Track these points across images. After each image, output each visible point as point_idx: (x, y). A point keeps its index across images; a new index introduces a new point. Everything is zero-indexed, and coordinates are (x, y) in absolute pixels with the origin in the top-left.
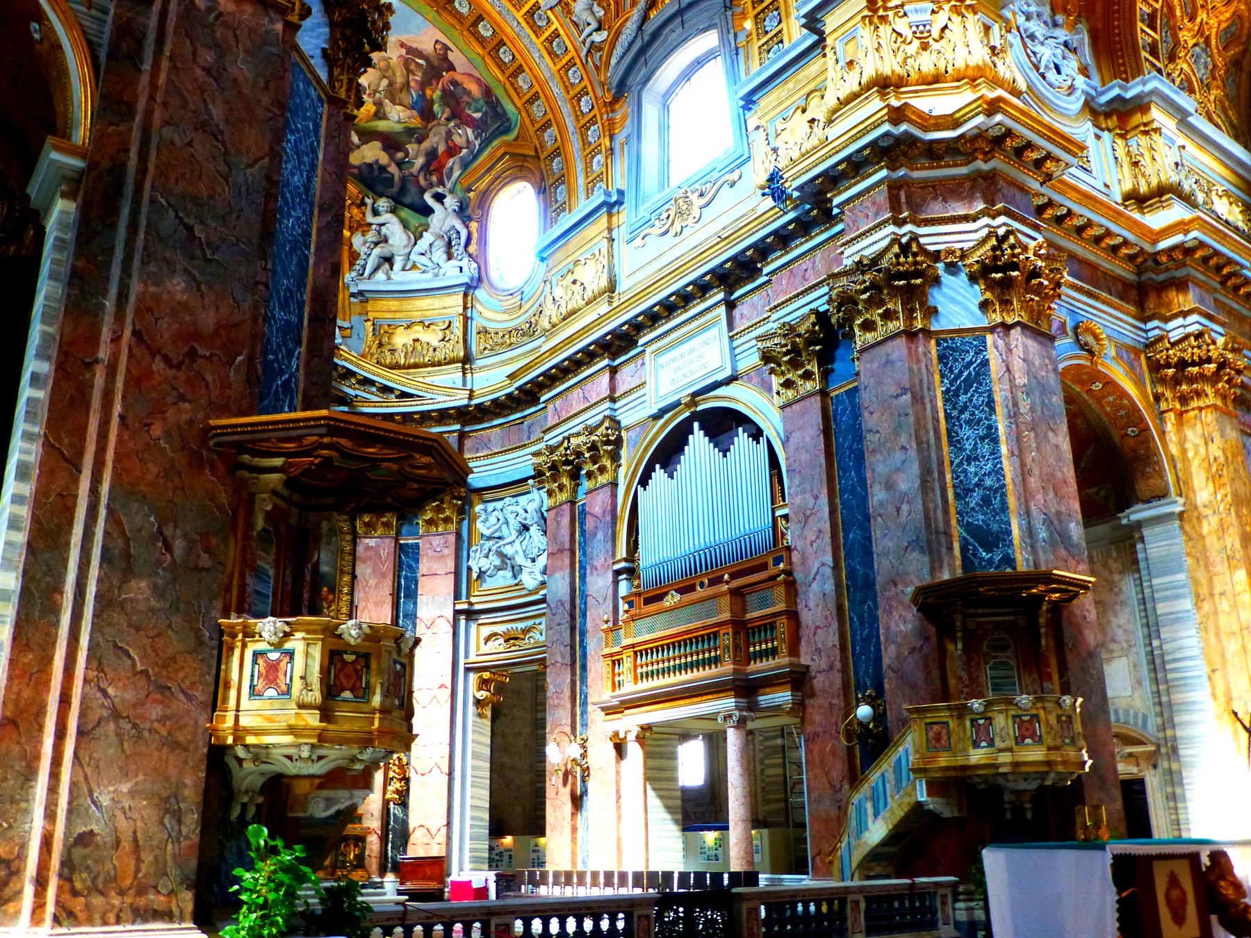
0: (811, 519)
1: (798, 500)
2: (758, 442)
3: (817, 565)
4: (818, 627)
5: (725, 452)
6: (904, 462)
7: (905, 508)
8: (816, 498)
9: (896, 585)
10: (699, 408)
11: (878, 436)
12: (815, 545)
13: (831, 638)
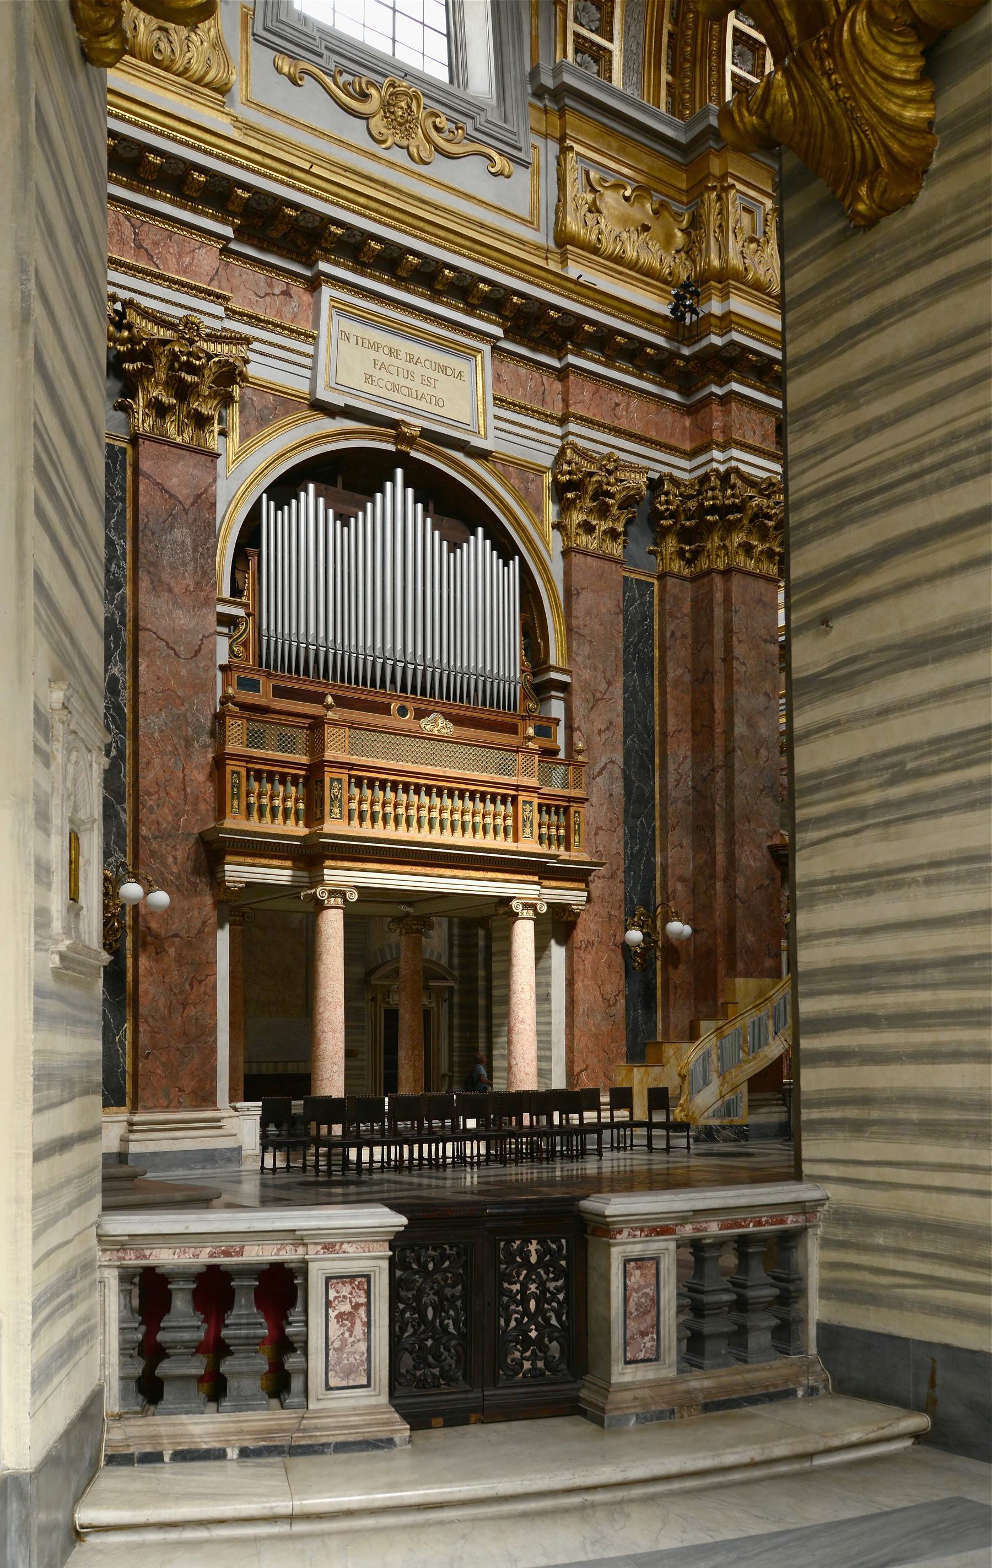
0: (601, 704)
1: (587, 674)
2: (506, 564)
3: (604, 760)
4: (599, 828)
5: (454, 546)
6: (766, 708)
7: (763, 752)
8: (609, 683)
9: (749, 822)
10: (414, 454)
11: (744, 668)
12: (603, 735)
13: (614, 845)
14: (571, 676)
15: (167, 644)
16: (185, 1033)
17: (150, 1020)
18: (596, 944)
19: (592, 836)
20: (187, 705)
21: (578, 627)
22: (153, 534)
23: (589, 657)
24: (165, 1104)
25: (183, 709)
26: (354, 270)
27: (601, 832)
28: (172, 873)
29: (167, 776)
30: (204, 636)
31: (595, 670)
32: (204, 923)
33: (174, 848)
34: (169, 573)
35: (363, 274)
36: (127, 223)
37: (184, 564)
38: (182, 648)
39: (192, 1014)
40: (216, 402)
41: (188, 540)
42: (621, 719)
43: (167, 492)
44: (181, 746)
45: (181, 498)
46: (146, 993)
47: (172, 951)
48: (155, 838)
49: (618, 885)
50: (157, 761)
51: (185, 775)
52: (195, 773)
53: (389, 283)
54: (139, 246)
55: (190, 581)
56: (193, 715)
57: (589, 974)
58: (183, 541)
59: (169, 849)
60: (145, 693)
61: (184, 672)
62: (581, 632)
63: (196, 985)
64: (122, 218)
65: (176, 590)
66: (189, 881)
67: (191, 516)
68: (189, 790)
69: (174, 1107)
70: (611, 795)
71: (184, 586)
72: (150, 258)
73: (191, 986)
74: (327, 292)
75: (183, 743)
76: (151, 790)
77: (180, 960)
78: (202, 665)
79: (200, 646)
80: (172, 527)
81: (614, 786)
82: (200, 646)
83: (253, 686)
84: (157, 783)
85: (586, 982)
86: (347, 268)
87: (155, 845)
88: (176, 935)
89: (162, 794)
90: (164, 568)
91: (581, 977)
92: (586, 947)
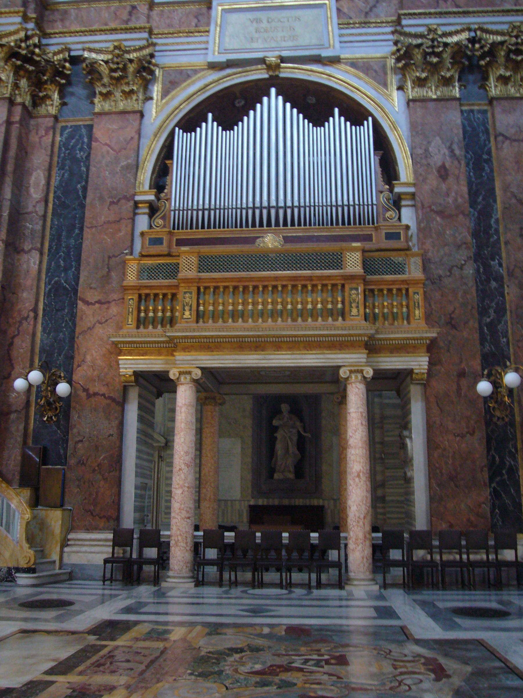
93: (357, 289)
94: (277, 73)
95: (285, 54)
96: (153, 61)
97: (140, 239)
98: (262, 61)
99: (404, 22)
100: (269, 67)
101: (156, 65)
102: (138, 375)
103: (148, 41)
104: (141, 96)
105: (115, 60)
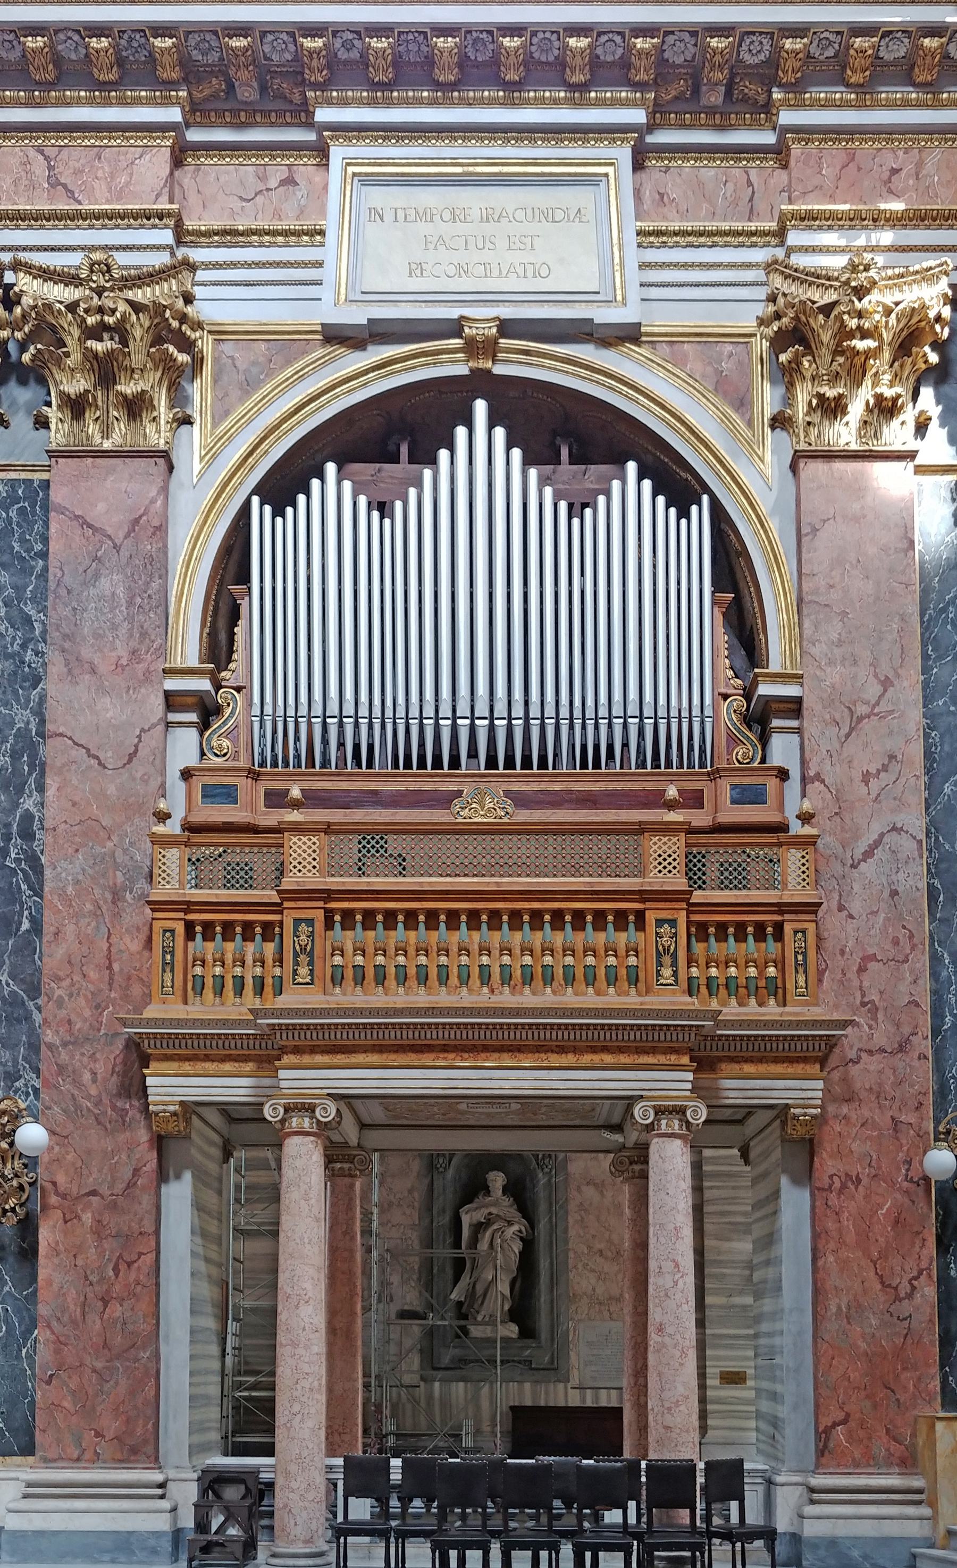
1: (834, 675)
3: (876, 828)
8: (886, 683)
12: (874, 784)
13: (903, 987)
14: (802, 685)
15: (88, 750)
16: (105, 1345)
17: (54, 1324)
18: (865, 1181)
19: (852, 975)
20: (115, 839)
21: (816, 591)
22: (69, 592)
23: (840, 643)
24: (75, 1456)
25: (110, 844)
26: (372, 103)
27: (873, 966)
28: (89, 1097)
29: (85, 949)
30: (143, 730)
31: (855, 663)
32: (136, 1172)
33: (92, 1057)
34: (93, 646)
35: (389, 103)
36: (41, 157)
37: (114, 627)
38: (110, 754)
39: (118, 1314)
40: (159, 374)
41: (121, 591)
42: (917, 750)
43: (90, 526)
44: (106, 902)
45: (110, 531)
46: (49, 1282)
47: (87, 1218)
48: (65, 1044)
49: (916, 1063)
50: (70, 930)
51: (110, 945)
52: (127, 939)
53: (433, 103)
54: (54, 182)
55: (122, 651)
56: (125, 851)
57: (851, 1237)
58: (113, 594)
59: (85, 1059)
60: (54, 829)
61: (112, 790)
62: (822, 599)
63: (123, 1267)
64: (32, 153)
65: (103, 668)
66: (114, 1108)
67: (125, 553)
68: (116, 967)
69: (88, 1461)
70: (894, 893)
71: (114, 660)
72: (70, 193)
73: (116, 1270)
74: (338, 153)
75: (109, 896)
76: (61, 974)
77: (99, 1230)
78: (139, 775)
79: (136, 746)
80: (97, 576)
81: (901, 876)
82: (136, 746)
83: (228, 794)
84: (69, 962)
85: (844, 1253)
86: (361, 103)
87: (64, 1056)
88: (94, 1193)
89: (76, 978)
90: (84, 639)
91: (832, 1245)
92: (844, 1186)
93: (673, 923)
94: (489, 364)
95: (507, 312)
96: (189, 310)
97: (182, 785)
98: (455, 328)
99: (794, 238)
100: (473, 348)
101: (198, 326)
102: (189, 1109)
103: (173, 254)
104: (164, 412)
105: (96, 301)
